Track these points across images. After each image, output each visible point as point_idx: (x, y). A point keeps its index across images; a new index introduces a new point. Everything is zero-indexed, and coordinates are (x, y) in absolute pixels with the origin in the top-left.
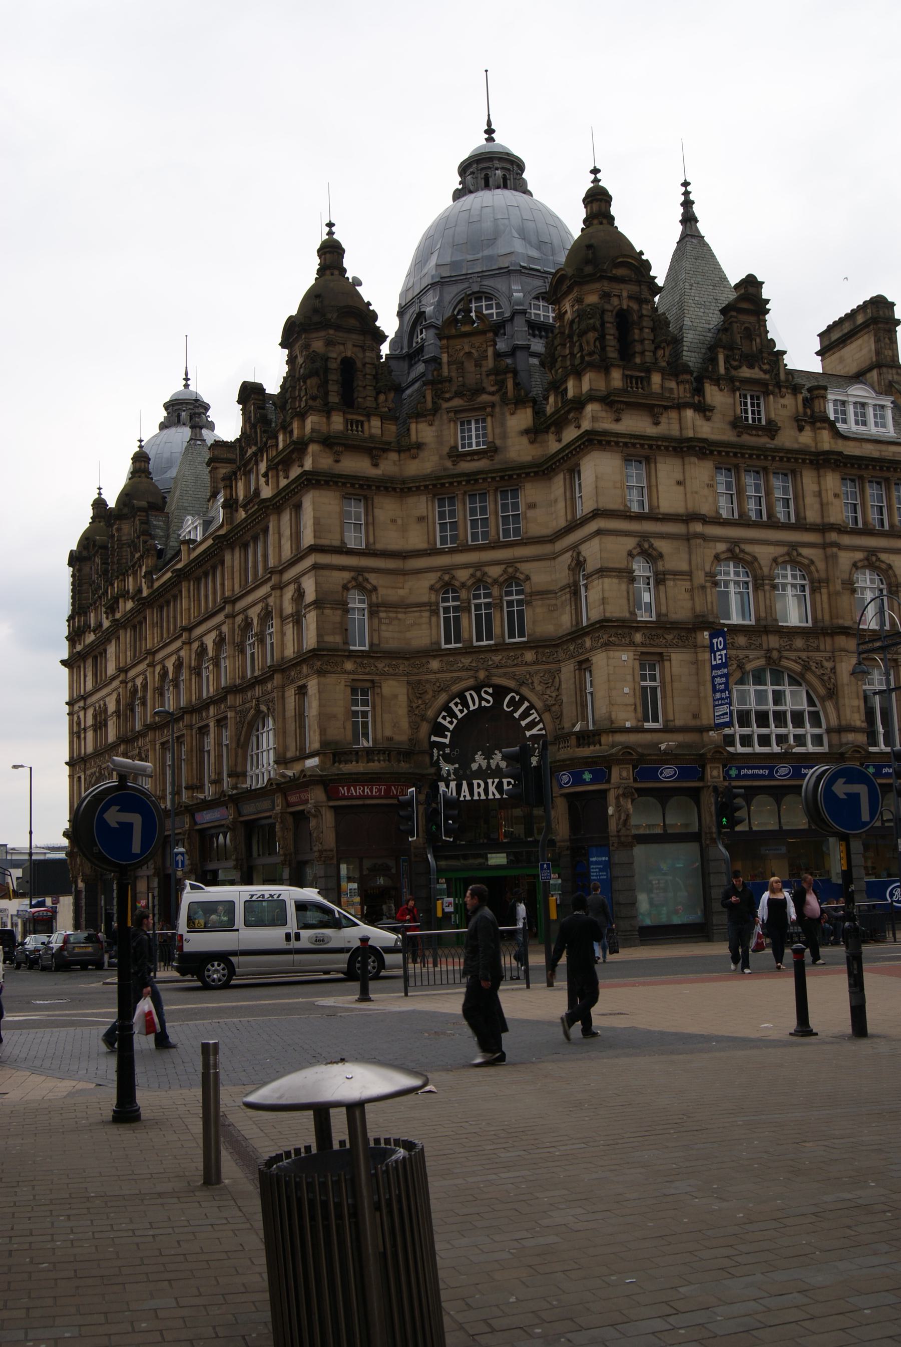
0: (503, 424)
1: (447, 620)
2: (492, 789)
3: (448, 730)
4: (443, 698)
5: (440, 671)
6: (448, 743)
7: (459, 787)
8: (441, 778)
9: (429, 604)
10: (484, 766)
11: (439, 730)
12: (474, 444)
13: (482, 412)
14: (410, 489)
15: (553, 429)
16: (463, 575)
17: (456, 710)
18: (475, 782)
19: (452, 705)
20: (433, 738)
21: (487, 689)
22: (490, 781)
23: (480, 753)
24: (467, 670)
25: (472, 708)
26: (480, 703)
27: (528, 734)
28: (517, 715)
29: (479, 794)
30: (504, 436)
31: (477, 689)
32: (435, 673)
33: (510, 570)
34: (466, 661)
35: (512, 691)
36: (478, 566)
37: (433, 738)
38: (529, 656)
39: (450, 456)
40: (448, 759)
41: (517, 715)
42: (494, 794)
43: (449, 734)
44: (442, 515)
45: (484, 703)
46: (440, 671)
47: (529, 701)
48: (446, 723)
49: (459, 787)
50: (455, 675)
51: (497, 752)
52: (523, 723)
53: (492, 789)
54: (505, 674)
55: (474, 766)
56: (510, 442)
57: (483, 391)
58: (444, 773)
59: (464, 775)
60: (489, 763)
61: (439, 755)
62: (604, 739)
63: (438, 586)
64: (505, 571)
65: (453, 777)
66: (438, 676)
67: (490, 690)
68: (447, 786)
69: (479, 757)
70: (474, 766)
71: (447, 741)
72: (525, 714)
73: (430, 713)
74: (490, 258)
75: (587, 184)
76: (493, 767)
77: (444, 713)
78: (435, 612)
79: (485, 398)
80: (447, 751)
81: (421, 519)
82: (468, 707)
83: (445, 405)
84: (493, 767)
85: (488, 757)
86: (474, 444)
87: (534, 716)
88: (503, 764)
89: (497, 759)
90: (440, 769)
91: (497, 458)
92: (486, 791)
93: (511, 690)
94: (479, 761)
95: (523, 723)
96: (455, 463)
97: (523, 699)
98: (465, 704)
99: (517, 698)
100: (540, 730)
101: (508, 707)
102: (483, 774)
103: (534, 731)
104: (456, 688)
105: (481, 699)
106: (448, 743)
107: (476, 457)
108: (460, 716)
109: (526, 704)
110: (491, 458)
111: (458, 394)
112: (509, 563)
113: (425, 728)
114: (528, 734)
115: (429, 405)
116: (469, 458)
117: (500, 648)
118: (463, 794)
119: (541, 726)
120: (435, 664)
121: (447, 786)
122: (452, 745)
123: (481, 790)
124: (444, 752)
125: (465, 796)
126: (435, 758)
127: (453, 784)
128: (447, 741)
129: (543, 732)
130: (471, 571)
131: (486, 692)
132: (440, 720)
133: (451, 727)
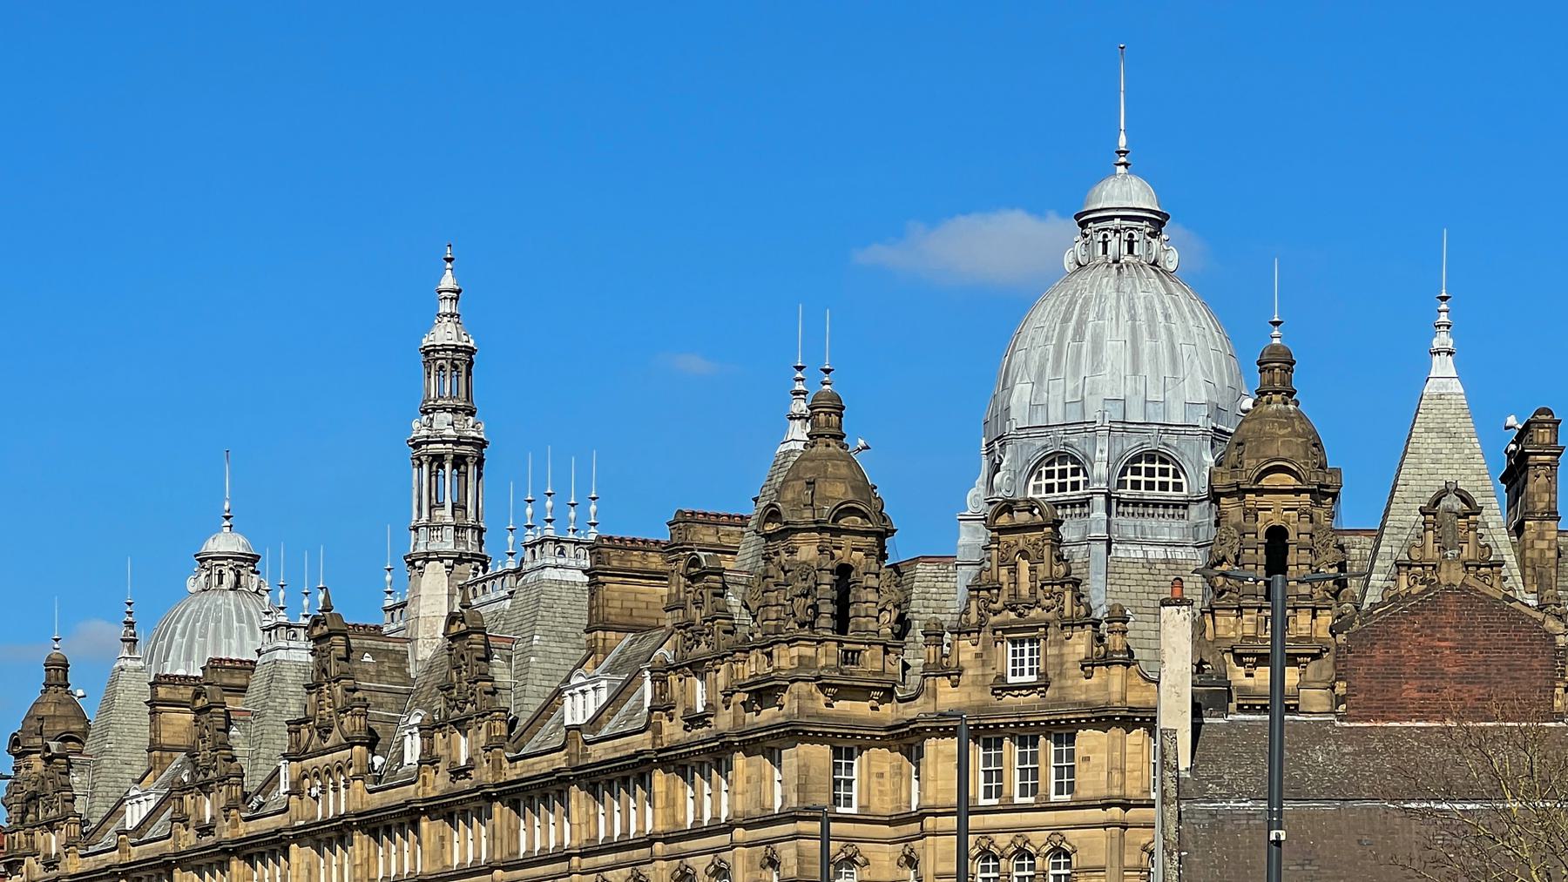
12: (1027, 671)
16: (1002, 840)
83: (993, 619)
86: (1027, 671)
107: (1024, 692)
115: (974, 618)
116: (1016, 692)
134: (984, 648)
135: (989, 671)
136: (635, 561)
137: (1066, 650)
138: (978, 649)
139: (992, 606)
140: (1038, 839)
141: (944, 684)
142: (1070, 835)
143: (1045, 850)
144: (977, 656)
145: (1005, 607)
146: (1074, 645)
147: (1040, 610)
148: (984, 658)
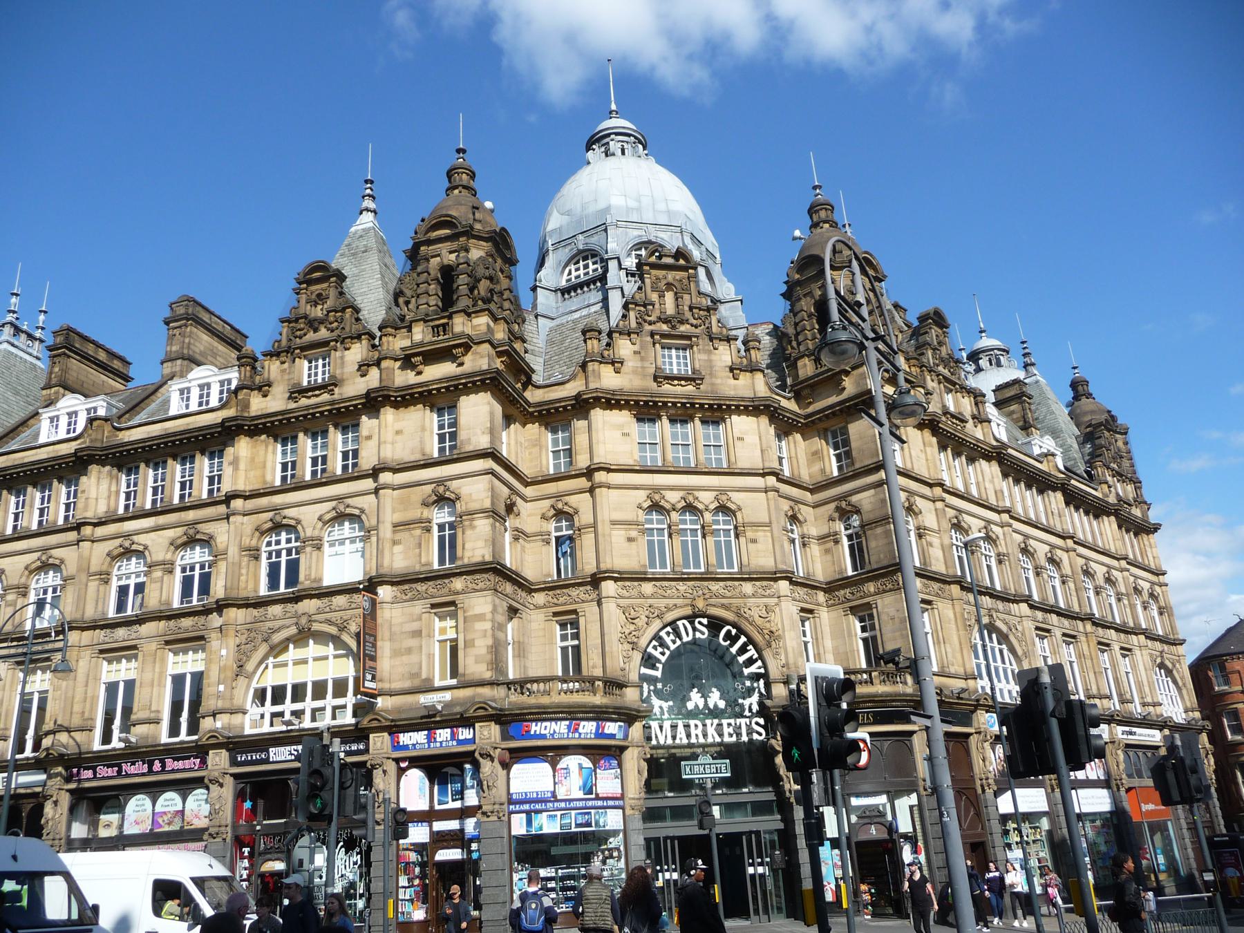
2: (711, 731)
3: (659, 661)
4: (657, 624)
5: (652, 596)
6: (659, 676)
7: (674, 727)
10: (701, 706)
11: (649, 661)
13: (686, 343)
14: (618, 401)
16: (673, 497)
17: (668, 640)
19: (663, 634)
21: (701, 620)
22: (708, 722)
23: (695, 690)
24: (685, 597)
25: (685, 639)
26: (694, 635)
27: (746, 671)
28: (734, 650)
29: (697, 735)
31: (691, 619)
32: (648, 598)
33: (724, 498)
34: (682, 586)
35: (728, 623)
36: (690, 490)
37: (644, 670)
38: (748, 588)
41: (734, 650)
42: (713, 738)
43: (660, 666)
45: (698, 635)
46: (652, 596)
47: (747, 636)
48: (657, 654)
49: (674, 727)
50: (671, 602)
51: (714, 690)
52: (741, 659)
53: (711, 731)
54: (723, 606)
57: (687, 321)
58: (656, 710)
60: (706, 701)
61: (649, 692)
63: (646, 505)
64: (716, 498)
65: (666, 716)
66: (650, 601)
67: (705, 621)
68: (661, 727)
70: (690, 706)
71: (658, 674)
72: (743, 650)
73: (643, 642)
76: (711, 706)
77: (654, 643)
80: (659, 686)
82: (681, 639)
83: (648, 328)
84: (711, 706)
85: (705, 696)
87: (752, 652)
88: (722, 704)
89: (715, 699)
93: (728, 623)
94: (695, 699)
95: (741, 659)
96: (659, 384)
97: (741, 631)
98: (678, 635)
99: (734, 632)
100: (759, 668)
101: (725, 640)
103: (753, 669)
104: (670, 617)
105: (694, 629)
106: (659, 676)
107: (683, 383)
108: (673, 647)
109: (743, 639)
110: (697, 386)
111: (660, 319)
112: (722, 491)
113: (637, 657)
114: (746, 671)
115: (634, 325)
116: (676, 382)
117: (708, 577)
118: (678, 736)
119: (759, 663)
121: (661, 727)
122: (665, 679)
123: (699, 731)
124: (655, 686)
125: (681, 739)
126: (645, 694)
127: (667, 725)
128: (658, 674)
129: (762, 671)
130: (681, 494)
131: (700, 623)
132: (650, 650)
133: (663, 659)
134: (642, 347)
135: (647, 364)
136: (90, 350)
137: (714, 357)
138: (636, 348)
139: (647, 318)
140: (706, 498)
141: (607, 371)
142: (736, 496)
143: (712, 507)
144: (635, 352)
145: (660, 319)
146: (721, 355)
147: (688, 326)
148: (643, 354)
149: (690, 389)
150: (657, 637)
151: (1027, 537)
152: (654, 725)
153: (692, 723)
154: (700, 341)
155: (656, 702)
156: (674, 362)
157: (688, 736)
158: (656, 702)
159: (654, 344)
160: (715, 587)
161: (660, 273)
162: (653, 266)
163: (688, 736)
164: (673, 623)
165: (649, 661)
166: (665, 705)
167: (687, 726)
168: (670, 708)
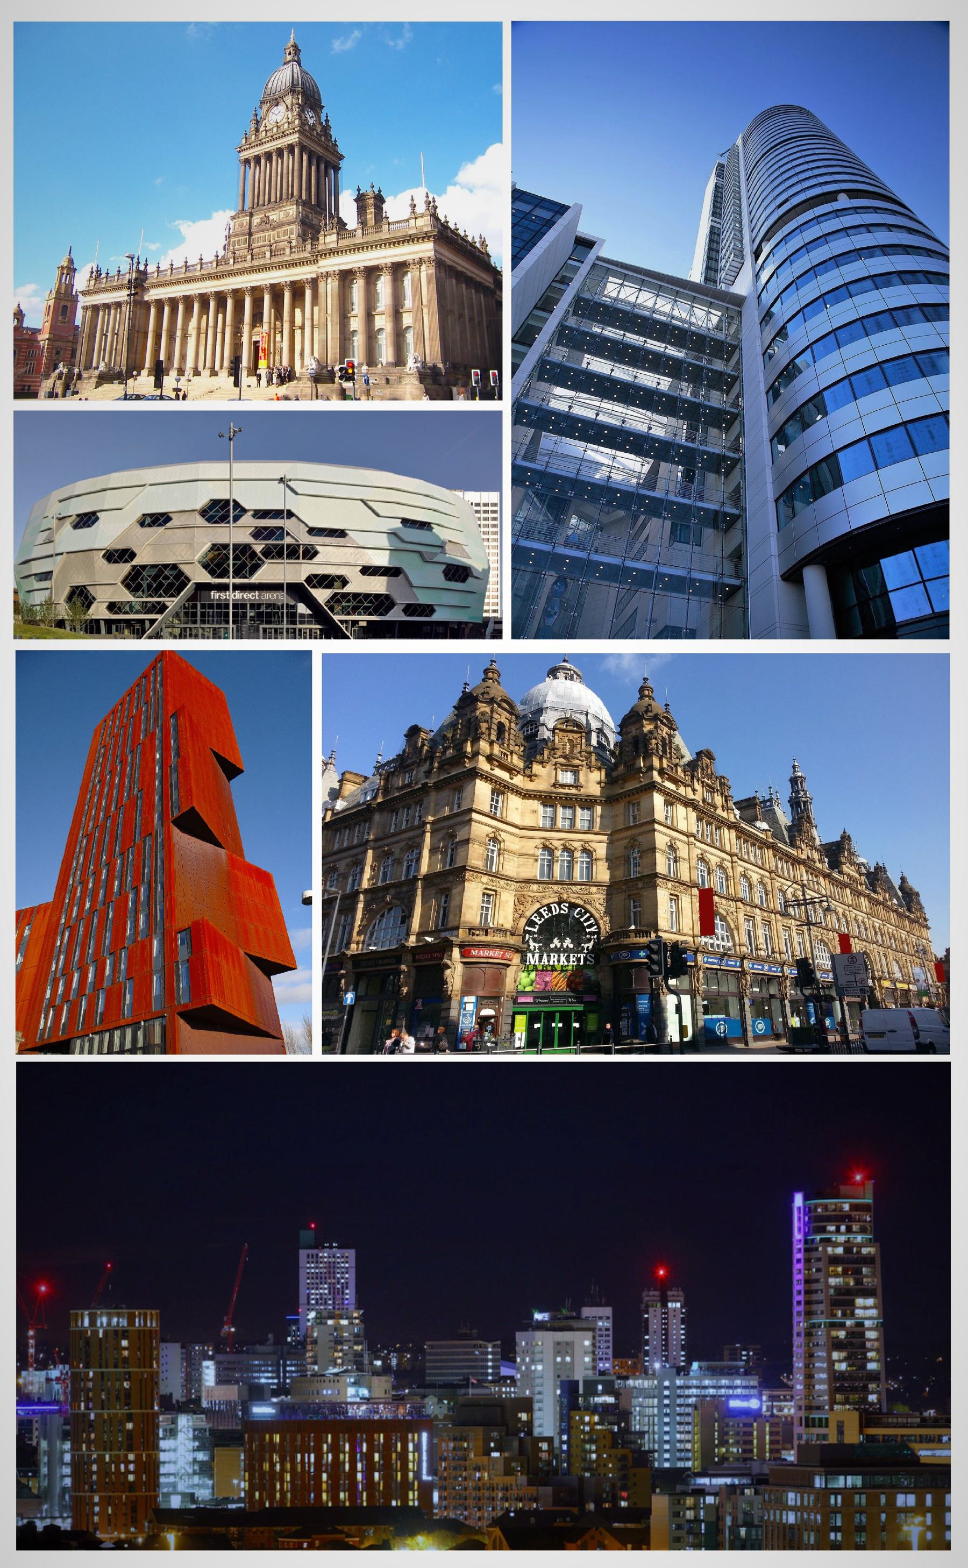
0: (587, 776)
1: (542, 865)
4: (537, 906)
7: (541, 958)
8: (530, 951)
9: (534, 855)
11: (531, 923)
15: (620, 782)
17: (544, 914)
18: (552, 955)
19: (541, 910)
20: (527, 928)
30: (587, 781)
31: (559, 903)
34: (556, 888)
37: (527, 928)
39: (554, 785)
40: (535, 940)
44: (545, 812)
49: (541, 958)
55: (552, 946)
56: (590, 785)
58: (532, 948)
59: (546, 948)
62: (653, 935)
69: (556, 941)
70: (552, 946)
71: (536, 930)
74: (578, 705)
75: (641, 683)
78: (536, 860)
79: (576, 762)
81: (534, 812)
83: (554, 761)
90: (529, 946)
91: (582, 790)
92: (559, 961)
98: (550, 910)
102: (557, 951)
104: (545, 902)
120: (535, 887)
122: (540, 932)
127: (537, 956)
128: (536, 930)
133: (539, 923)
149: (573, 791)
150: (537, 911)
151: (746, 869)
152: (529, 955)
153: (552, 955)
154: (584, 769)
155: (532, 943)
156: (567, 778)
157: (549, 961)
158: (532, 943)
159: (556, 769)
160: (574, 888)
161: (565, 734)
162: (561, 730)
163: (549, 961)
164: (548, 906)
165: (531, 923)
166: (537, 945)
167: (549, 956)
168: (540, 948)
